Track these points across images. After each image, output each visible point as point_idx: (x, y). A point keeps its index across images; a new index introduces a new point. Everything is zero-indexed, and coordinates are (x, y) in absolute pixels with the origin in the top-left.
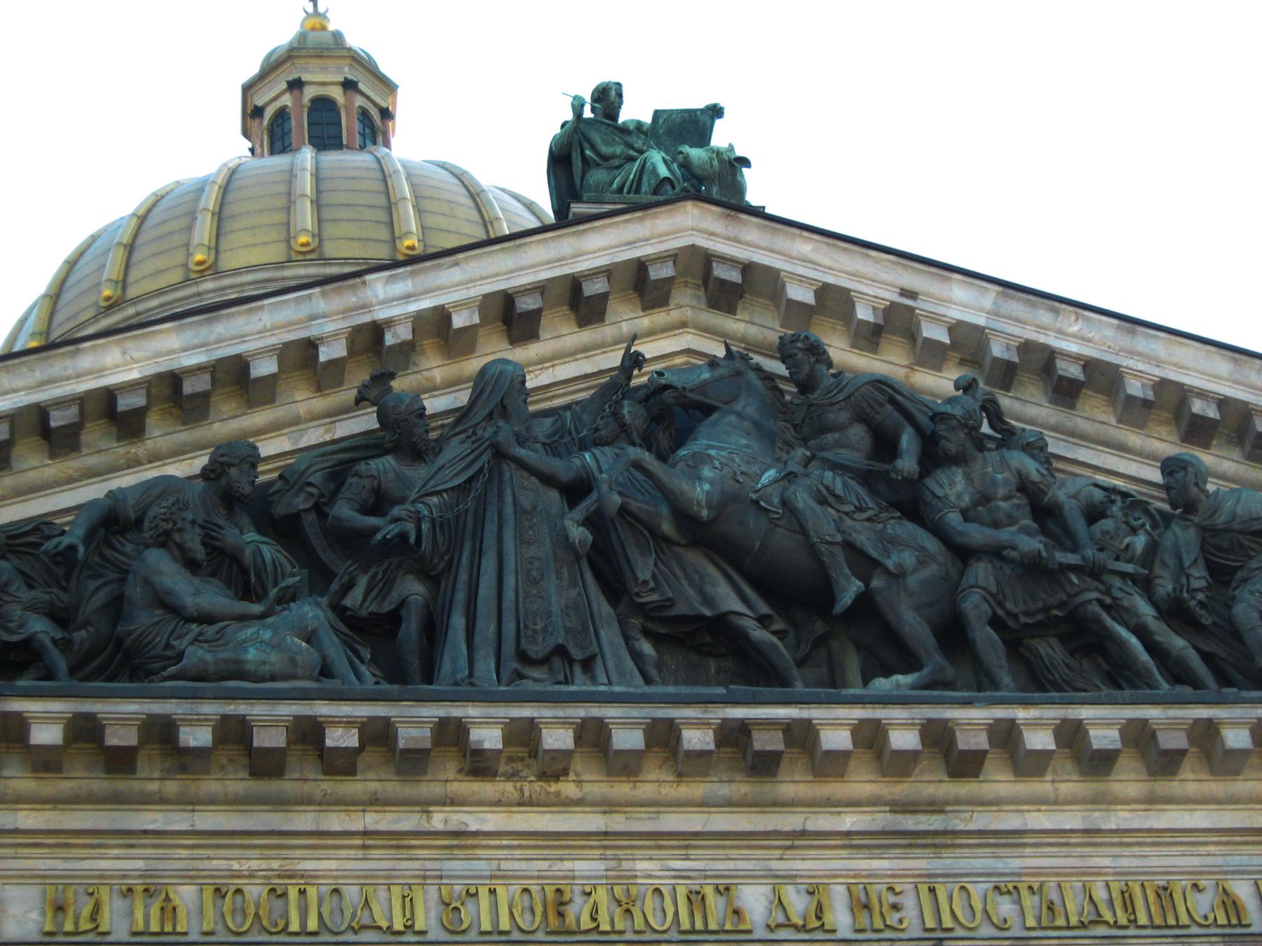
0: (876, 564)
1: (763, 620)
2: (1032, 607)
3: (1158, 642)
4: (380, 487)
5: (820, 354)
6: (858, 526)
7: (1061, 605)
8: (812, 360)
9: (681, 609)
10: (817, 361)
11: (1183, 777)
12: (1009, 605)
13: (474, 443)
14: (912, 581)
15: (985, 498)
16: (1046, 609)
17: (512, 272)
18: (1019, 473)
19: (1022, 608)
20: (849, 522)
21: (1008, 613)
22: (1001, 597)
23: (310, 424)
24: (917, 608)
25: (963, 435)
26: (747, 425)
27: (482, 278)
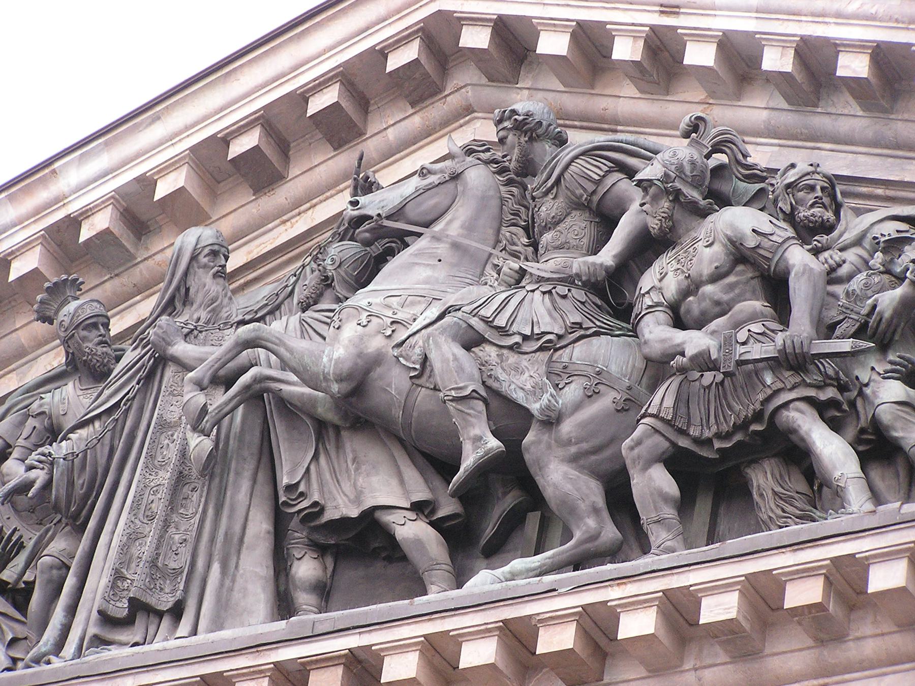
0: (527, 414)
1: (420, 508)
2: (725, 428)
3: (896, 438)
4: (52, 424)
5: (532, 130)
6: (524, 361)
7: (758, 416)
8: (523, 139)
9: (330, 514)
10: (531, 139)
11: (858, 634)
12: (694, 432)
13: (144, 347)
14: (567, 427)
15: (692, 288)
16: (743, 426)
17: (222, 109)
18: (732, 242)
19: (714, 429)
20: (512, 358)
21: (697, 441)
22: (679, 424)
23: (40, 351)
24: (574, 460)
25: (667, 205)
26: (442, 249)
27: (187, 128)
